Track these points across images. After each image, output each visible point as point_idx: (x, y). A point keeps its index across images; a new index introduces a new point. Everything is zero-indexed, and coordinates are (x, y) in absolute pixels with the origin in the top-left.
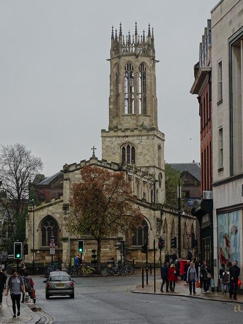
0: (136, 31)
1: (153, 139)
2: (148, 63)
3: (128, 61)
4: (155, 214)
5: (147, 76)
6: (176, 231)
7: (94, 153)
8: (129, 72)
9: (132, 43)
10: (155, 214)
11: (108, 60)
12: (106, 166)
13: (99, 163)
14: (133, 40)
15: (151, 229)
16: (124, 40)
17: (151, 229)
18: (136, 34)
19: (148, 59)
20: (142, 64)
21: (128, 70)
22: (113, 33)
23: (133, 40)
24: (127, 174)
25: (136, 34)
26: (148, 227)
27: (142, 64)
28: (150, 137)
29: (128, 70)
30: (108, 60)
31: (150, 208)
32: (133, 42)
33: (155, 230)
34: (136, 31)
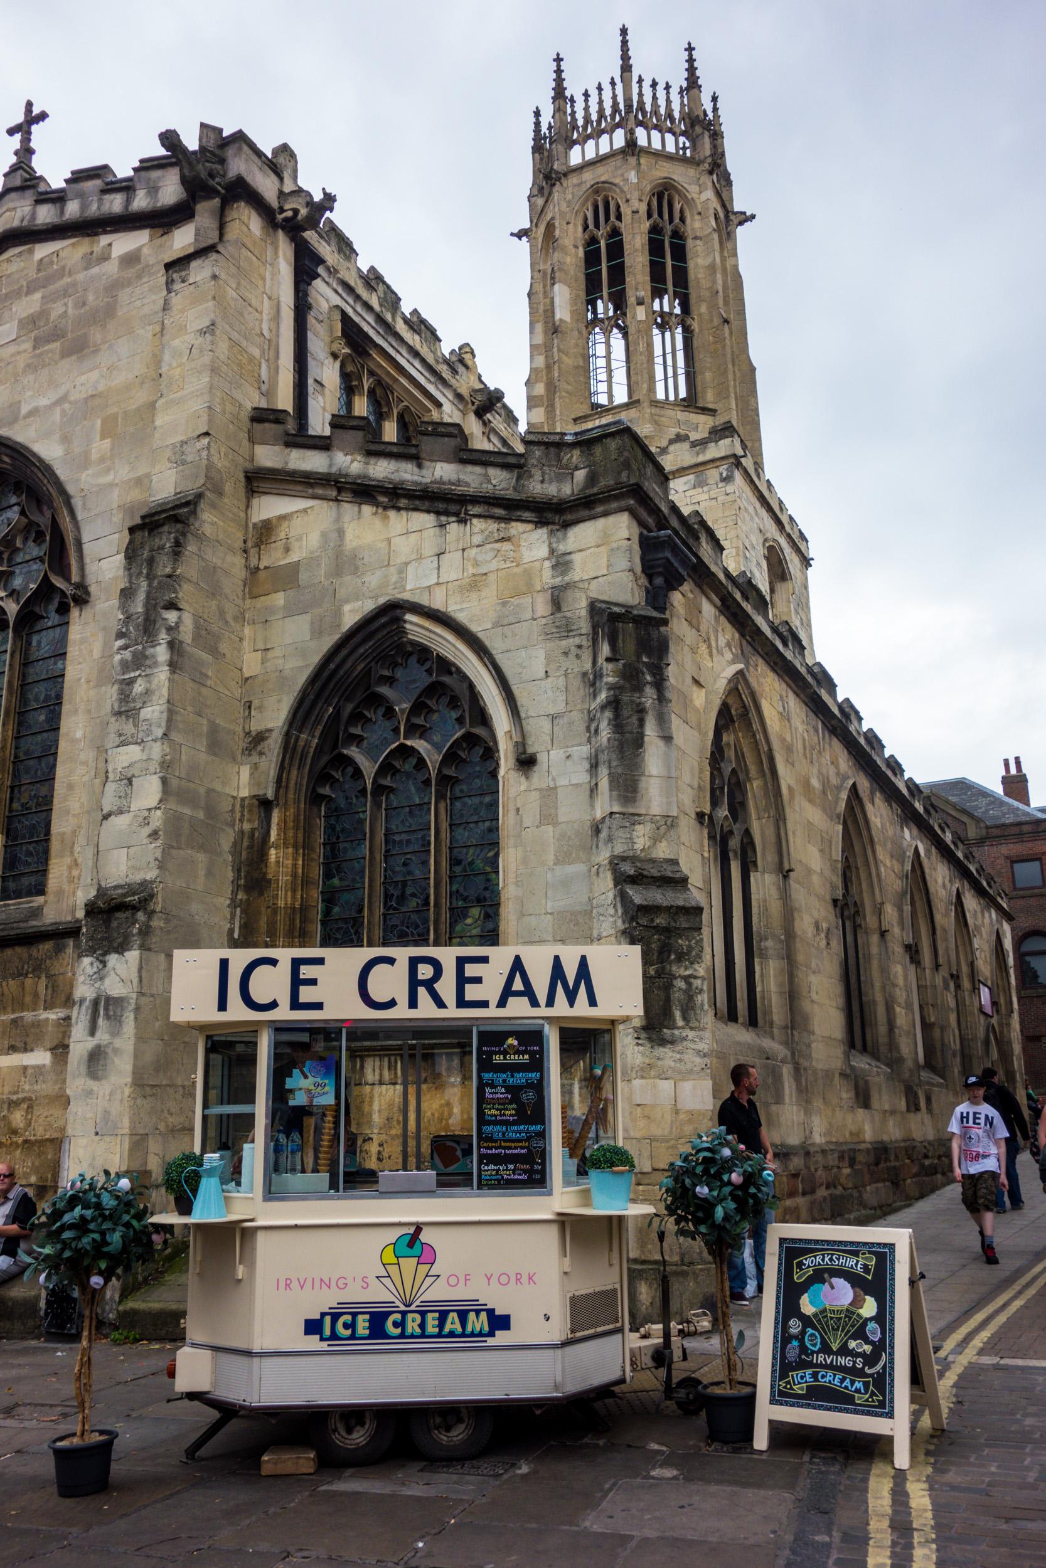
0: (625, 57)
1: (728, 479)
2: (692, 190)
3: (597, 189)
4: (561, 563)
5: (690, 243)
6: (890, 910)
7: (26, 152)
8: (602, 233)
9: (608, 112)
10: (561, 563)
11: (520, 235)
12: (93, 210)
13: (45, 215)
14: (614, 97)
15: (526, 762)
16: (573, 113)
17: (526, 762)
18: (626, 68)
19: (692, 172)
20: (664, 196)
21: (597, 226)
22: (537, 124)
23: (614, 97)
24: (306, 267)
25: (626, 68)
26: (490, 753)
27: (664, 196)
28: (713, 475)
29: (597, 226)
30: (520, 235)
31: (509, 508)
32: (615, 105)
33: (566, 764)
34: (625, 57)
